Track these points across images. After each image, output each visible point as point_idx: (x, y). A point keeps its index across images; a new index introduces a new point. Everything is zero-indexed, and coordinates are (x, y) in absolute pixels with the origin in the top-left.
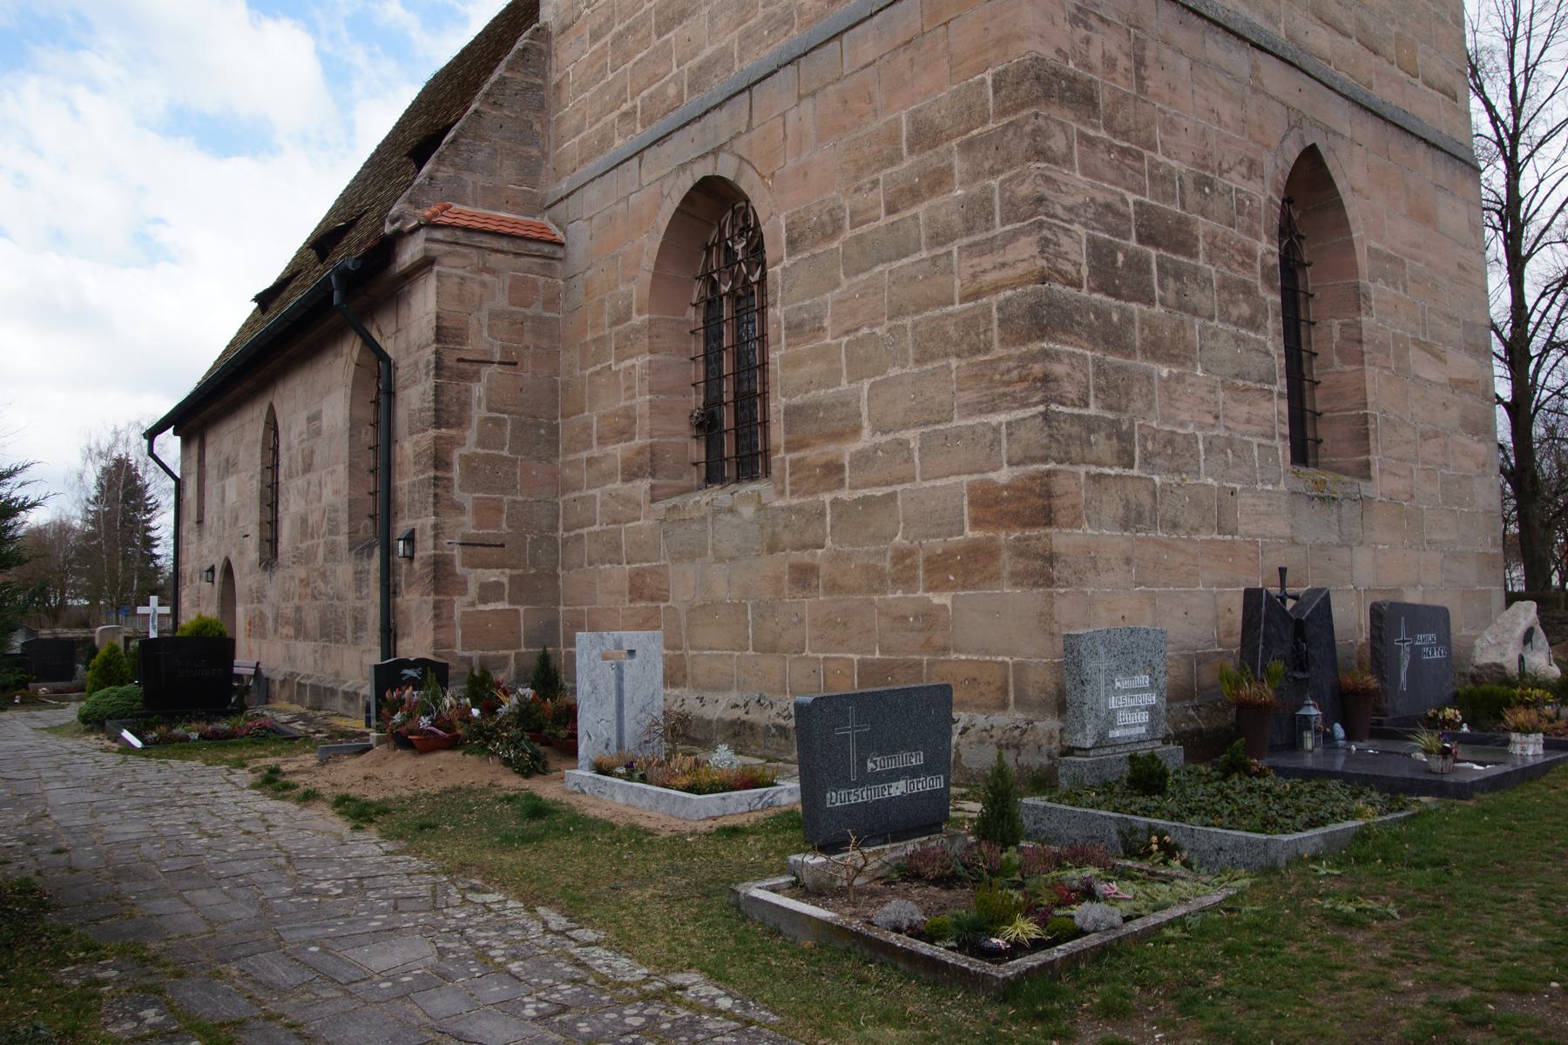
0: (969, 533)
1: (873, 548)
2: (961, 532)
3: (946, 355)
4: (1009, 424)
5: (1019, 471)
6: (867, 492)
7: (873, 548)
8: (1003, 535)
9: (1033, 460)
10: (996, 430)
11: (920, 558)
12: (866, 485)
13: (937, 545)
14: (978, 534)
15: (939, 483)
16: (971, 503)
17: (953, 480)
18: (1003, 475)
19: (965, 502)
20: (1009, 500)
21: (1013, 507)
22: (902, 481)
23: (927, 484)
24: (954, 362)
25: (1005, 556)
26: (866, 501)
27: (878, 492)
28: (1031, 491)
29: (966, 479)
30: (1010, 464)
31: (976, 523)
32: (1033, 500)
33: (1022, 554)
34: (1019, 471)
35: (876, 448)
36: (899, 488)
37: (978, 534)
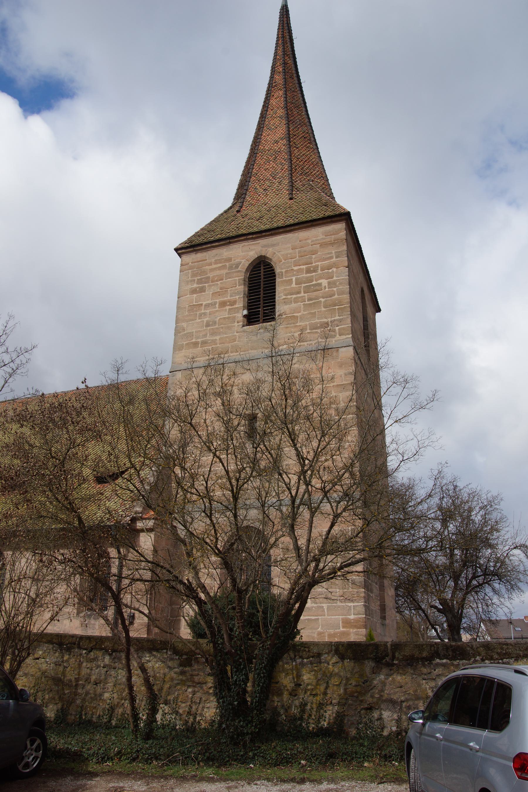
0: (342, 629)
1: (311, 631)
2: (339, 629)
3: (336, 588)
4: (354, 606)
5: (356, 616)
6: (309, 617)
7: (311, 631)
8: (351, 630)
9: (360, 614)
10: (350, 607)
11: (326, 634)
12: (309, 616)
13: (332, 631)
14: (344, 629)
15: (333, 617)
16: (342, 622)
17: (337, 617)
18: (352, 617)
19: (341, 622)
20: (354, 622)
21: (354, 624)
22: (321, 616)
23: (329, 617)
24: (338, 590)
25: (352, 635)
26: (308, 619)
27: (313, 618)
28: (360, 621)
29: (341, 617)
30: (354, 614)
31: (343, 627)
32: (360, 623)
33: (357, 634)
34: (356, 616)
35: (312, 607)
36: (320, 617)
37: (344, 629)
